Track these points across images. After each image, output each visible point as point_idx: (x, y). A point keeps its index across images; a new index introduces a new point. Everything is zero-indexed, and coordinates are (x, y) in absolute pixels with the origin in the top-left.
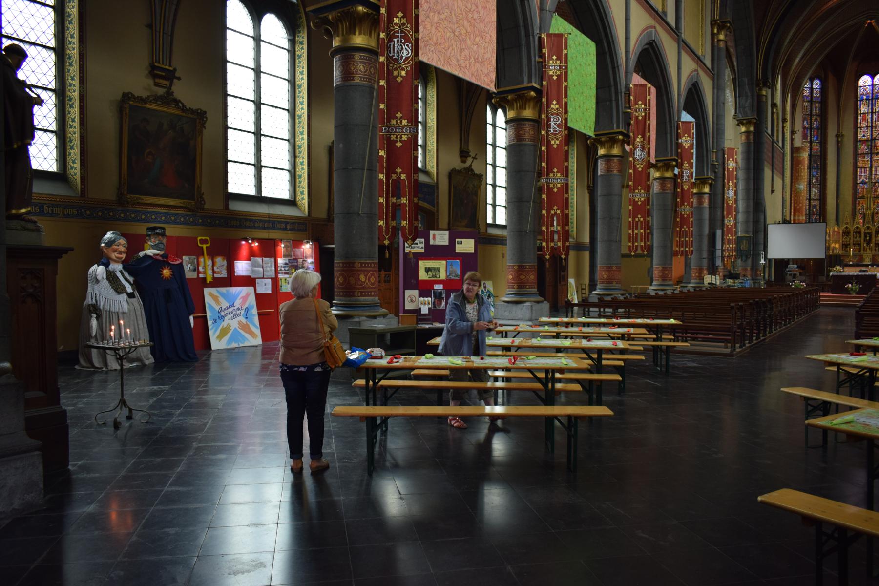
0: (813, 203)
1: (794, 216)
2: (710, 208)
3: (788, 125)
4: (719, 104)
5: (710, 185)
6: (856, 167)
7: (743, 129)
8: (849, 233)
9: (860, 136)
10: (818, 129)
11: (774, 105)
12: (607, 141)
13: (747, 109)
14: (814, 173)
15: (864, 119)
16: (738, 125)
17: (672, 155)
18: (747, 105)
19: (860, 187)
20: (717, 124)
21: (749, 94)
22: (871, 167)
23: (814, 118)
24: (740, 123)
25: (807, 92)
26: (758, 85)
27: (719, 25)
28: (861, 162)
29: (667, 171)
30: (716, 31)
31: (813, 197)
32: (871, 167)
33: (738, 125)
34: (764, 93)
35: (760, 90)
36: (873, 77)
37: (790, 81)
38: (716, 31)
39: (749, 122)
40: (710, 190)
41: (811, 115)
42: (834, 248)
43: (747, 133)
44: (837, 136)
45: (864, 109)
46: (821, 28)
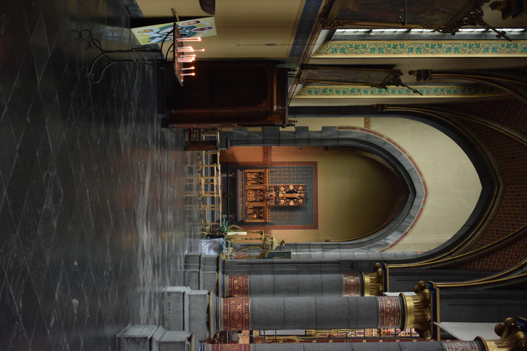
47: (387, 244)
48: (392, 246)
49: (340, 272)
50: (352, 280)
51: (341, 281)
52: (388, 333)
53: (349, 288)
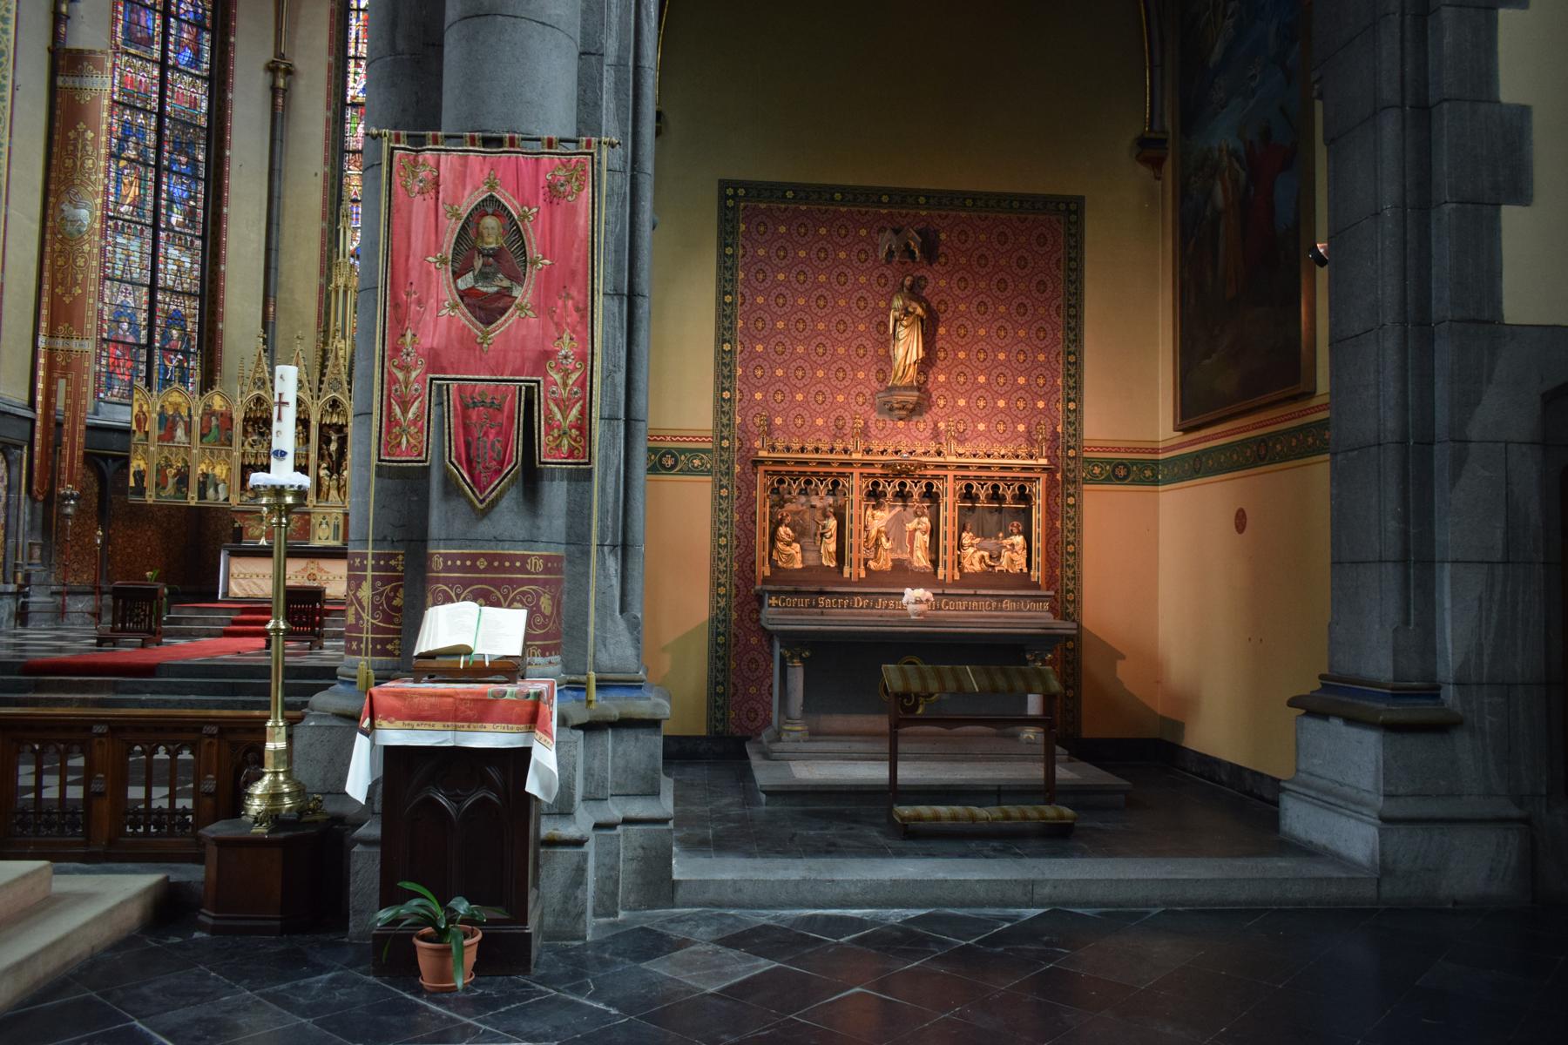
1: (52, 335)
31: (167, 278)
42: (206, 482)
44: (272, 69)
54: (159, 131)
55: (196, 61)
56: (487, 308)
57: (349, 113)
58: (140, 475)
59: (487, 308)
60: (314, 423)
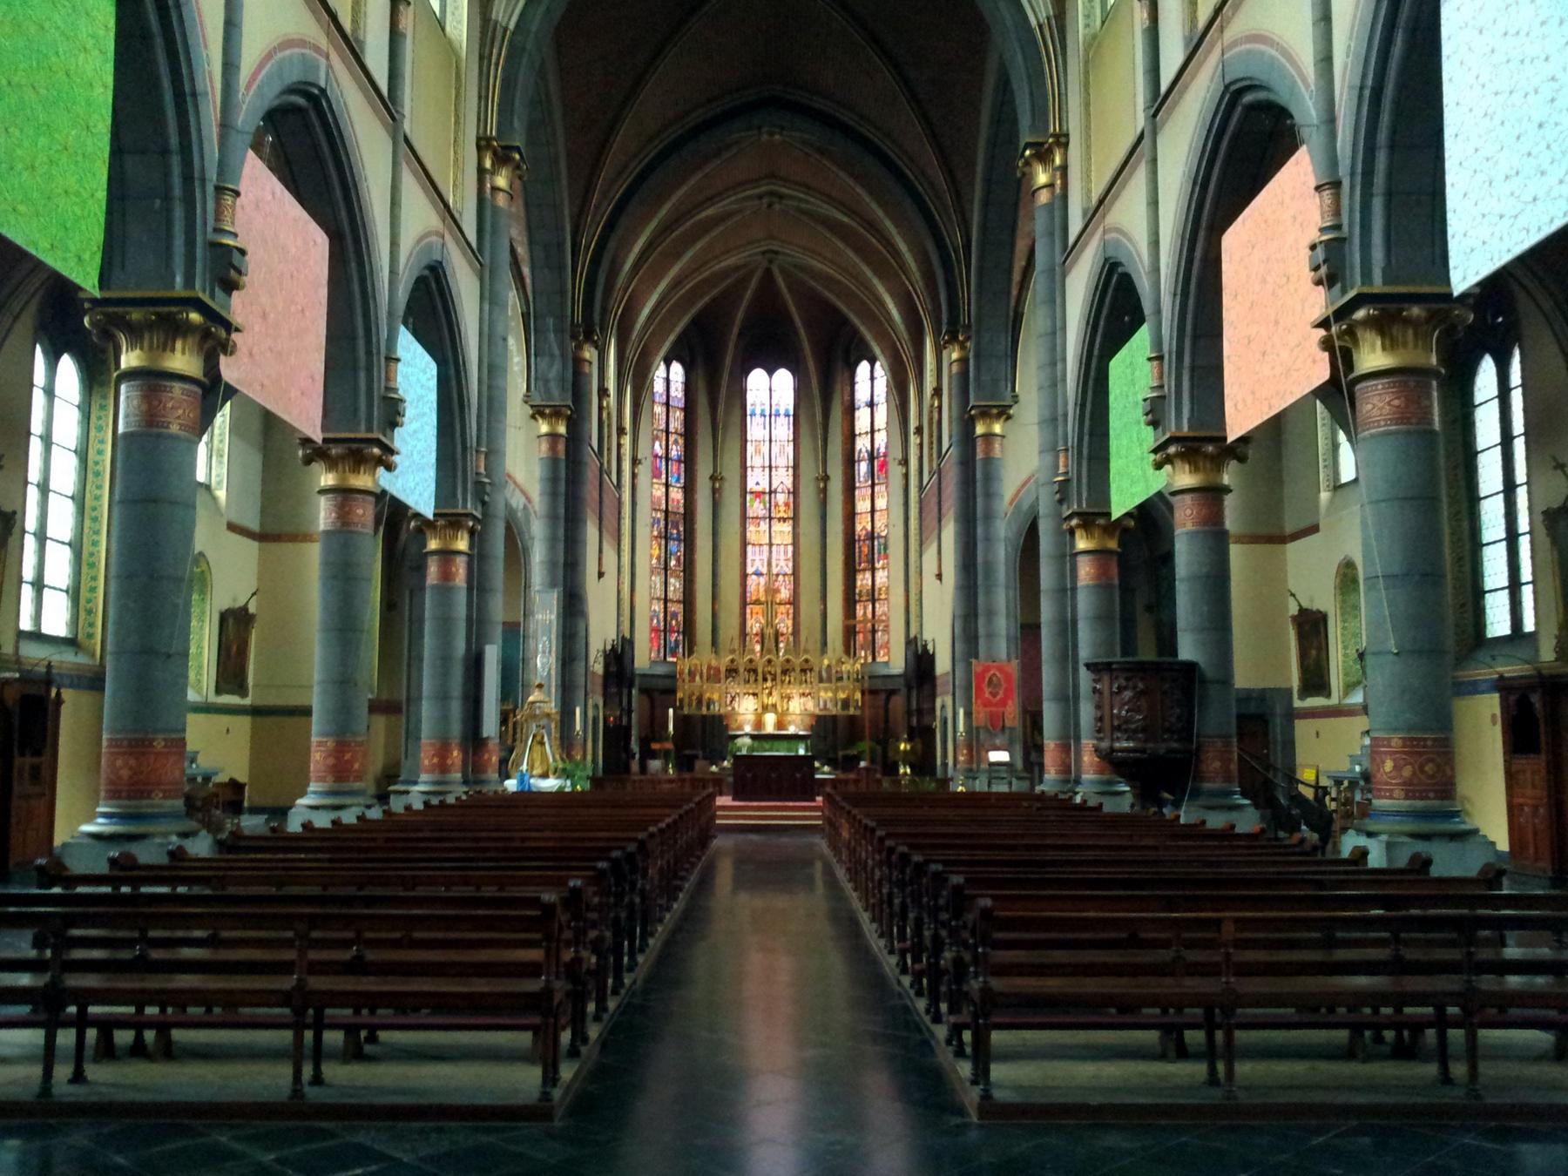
0: (672, 608)
2: (470, 589)
3: (627, 441)
4: (491, 339)
5: (472, 532)
6: (744, 544)
7: (544, 428)
8: (736, 671)
9: (751, 485)
10: (679, 461)
11: (603, 392)
12: (150, 326)
13: (553, 385)
14: (673, 546)
15: (758, 451)
16: (533, 417)
17: (370, 429)
18: (553, 373)
19: (752, 581)
20: (489, 387)
21: (557, 352)
22: (771, 545)
23: (672, 438)
24: (538, 412)
25: (659, 386)
26: (574, 337)
27: (495, 153)
28: (752, 534)
29: (355, 470)
30: (488, 164)
31: (670, 595)
32: (771, 545)
33: (533, 417)
34: (587, 355)
35: (579, 347)
36: (770, 373)
37: (632, 354)
38: (488, 164)
39: (556, 414)
40: (471, 546)
41: (667, 432)
43: (553, 436)
44: (713, 478)
45: (756, 430)
46: (689, 254)
47: (525, 507)
48: (528, 499)
49: (423, 589)
50: (433, 569)
51: (433, 587)
52: (787, 505)
53: (446, 575)
54: (666, 519)
55: (678, 480)
56: (994, 695)
57: (748, 497)
58: (681, 700)
59: (994, 695)
60: (760, 671)
